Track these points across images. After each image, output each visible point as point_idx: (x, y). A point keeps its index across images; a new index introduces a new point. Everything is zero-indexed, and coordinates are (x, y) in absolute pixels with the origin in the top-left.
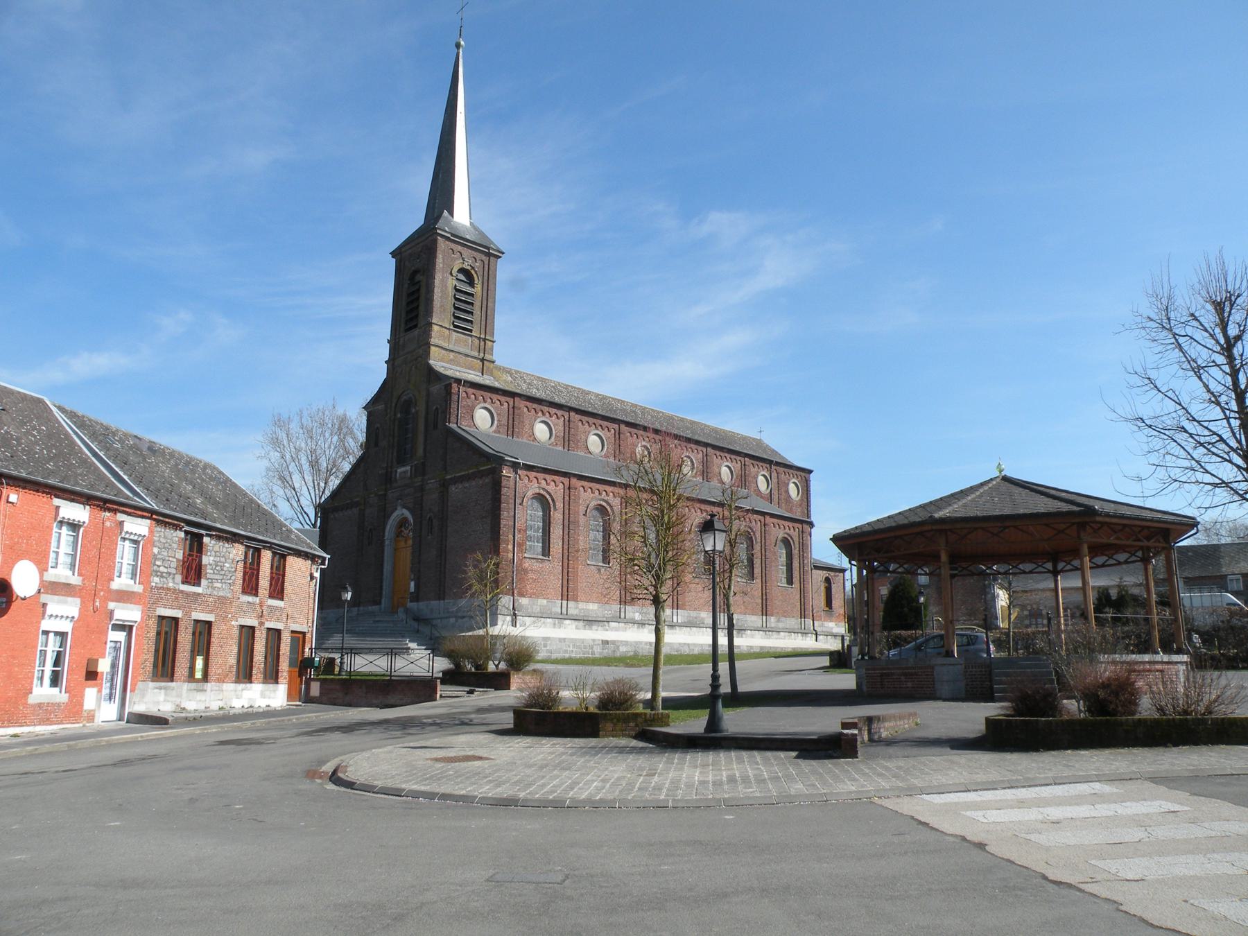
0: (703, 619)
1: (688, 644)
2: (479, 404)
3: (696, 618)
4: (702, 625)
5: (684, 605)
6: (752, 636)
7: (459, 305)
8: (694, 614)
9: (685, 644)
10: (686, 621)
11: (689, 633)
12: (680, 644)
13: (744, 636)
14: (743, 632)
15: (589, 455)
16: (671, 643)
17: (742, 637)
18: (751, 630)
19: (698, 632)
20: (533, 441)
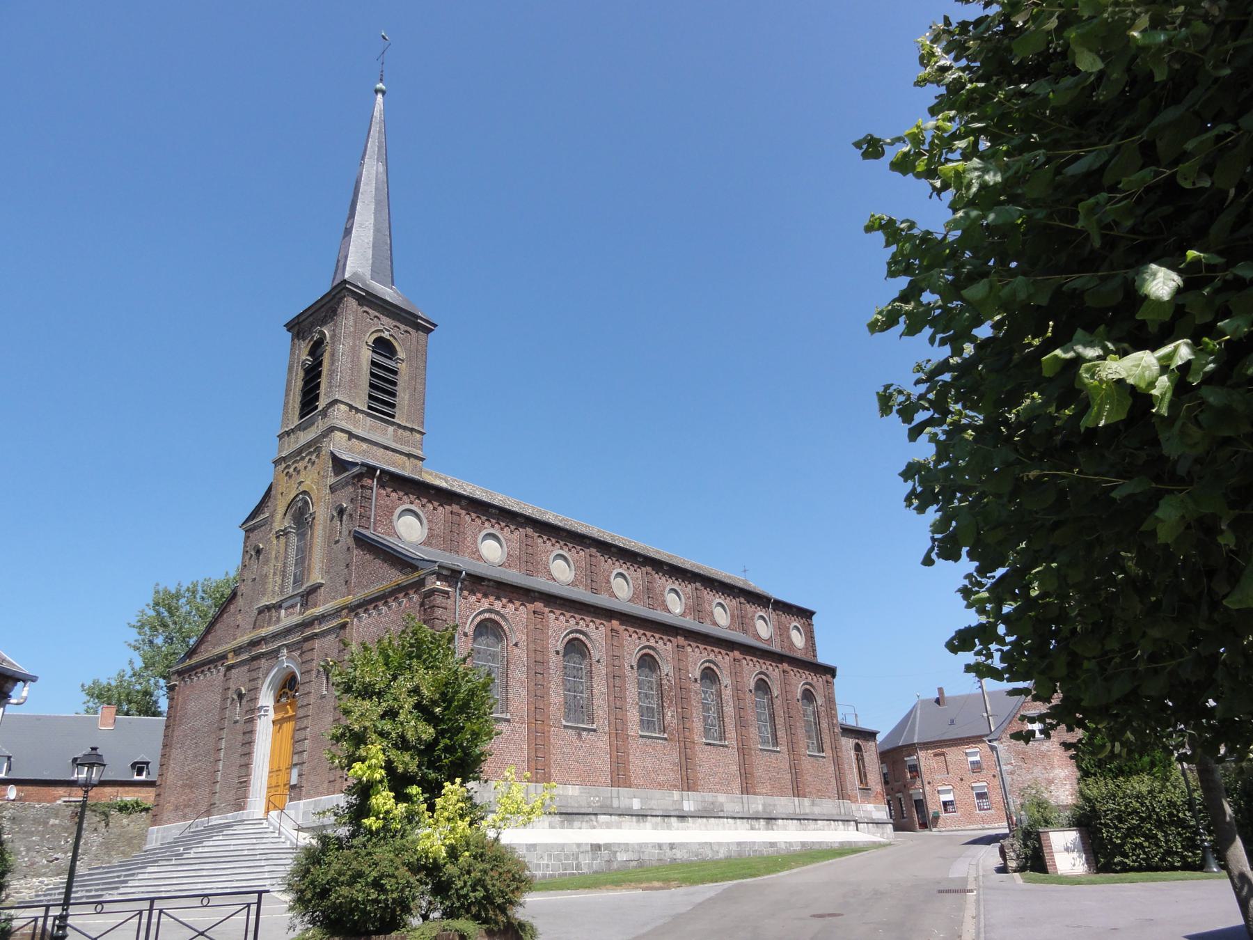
0: (722, 804)
1: (711, 843)
2: (402, 504)
3: (712, 803)
4: (721, 814)
5: (695, 784)
6: (785, 828)
7: (377, 371)
8: (709, 797)
9: (706, 843)
10: (700, 808)
11: (706, 826)
12: (700, 844)
13: (775, 827)
14: (773, 821)
15: (551, 582)
16: (687, 843)
17: (773, 829)
18: (783, 819)
19: (718, 825)
20: (478, 559)
